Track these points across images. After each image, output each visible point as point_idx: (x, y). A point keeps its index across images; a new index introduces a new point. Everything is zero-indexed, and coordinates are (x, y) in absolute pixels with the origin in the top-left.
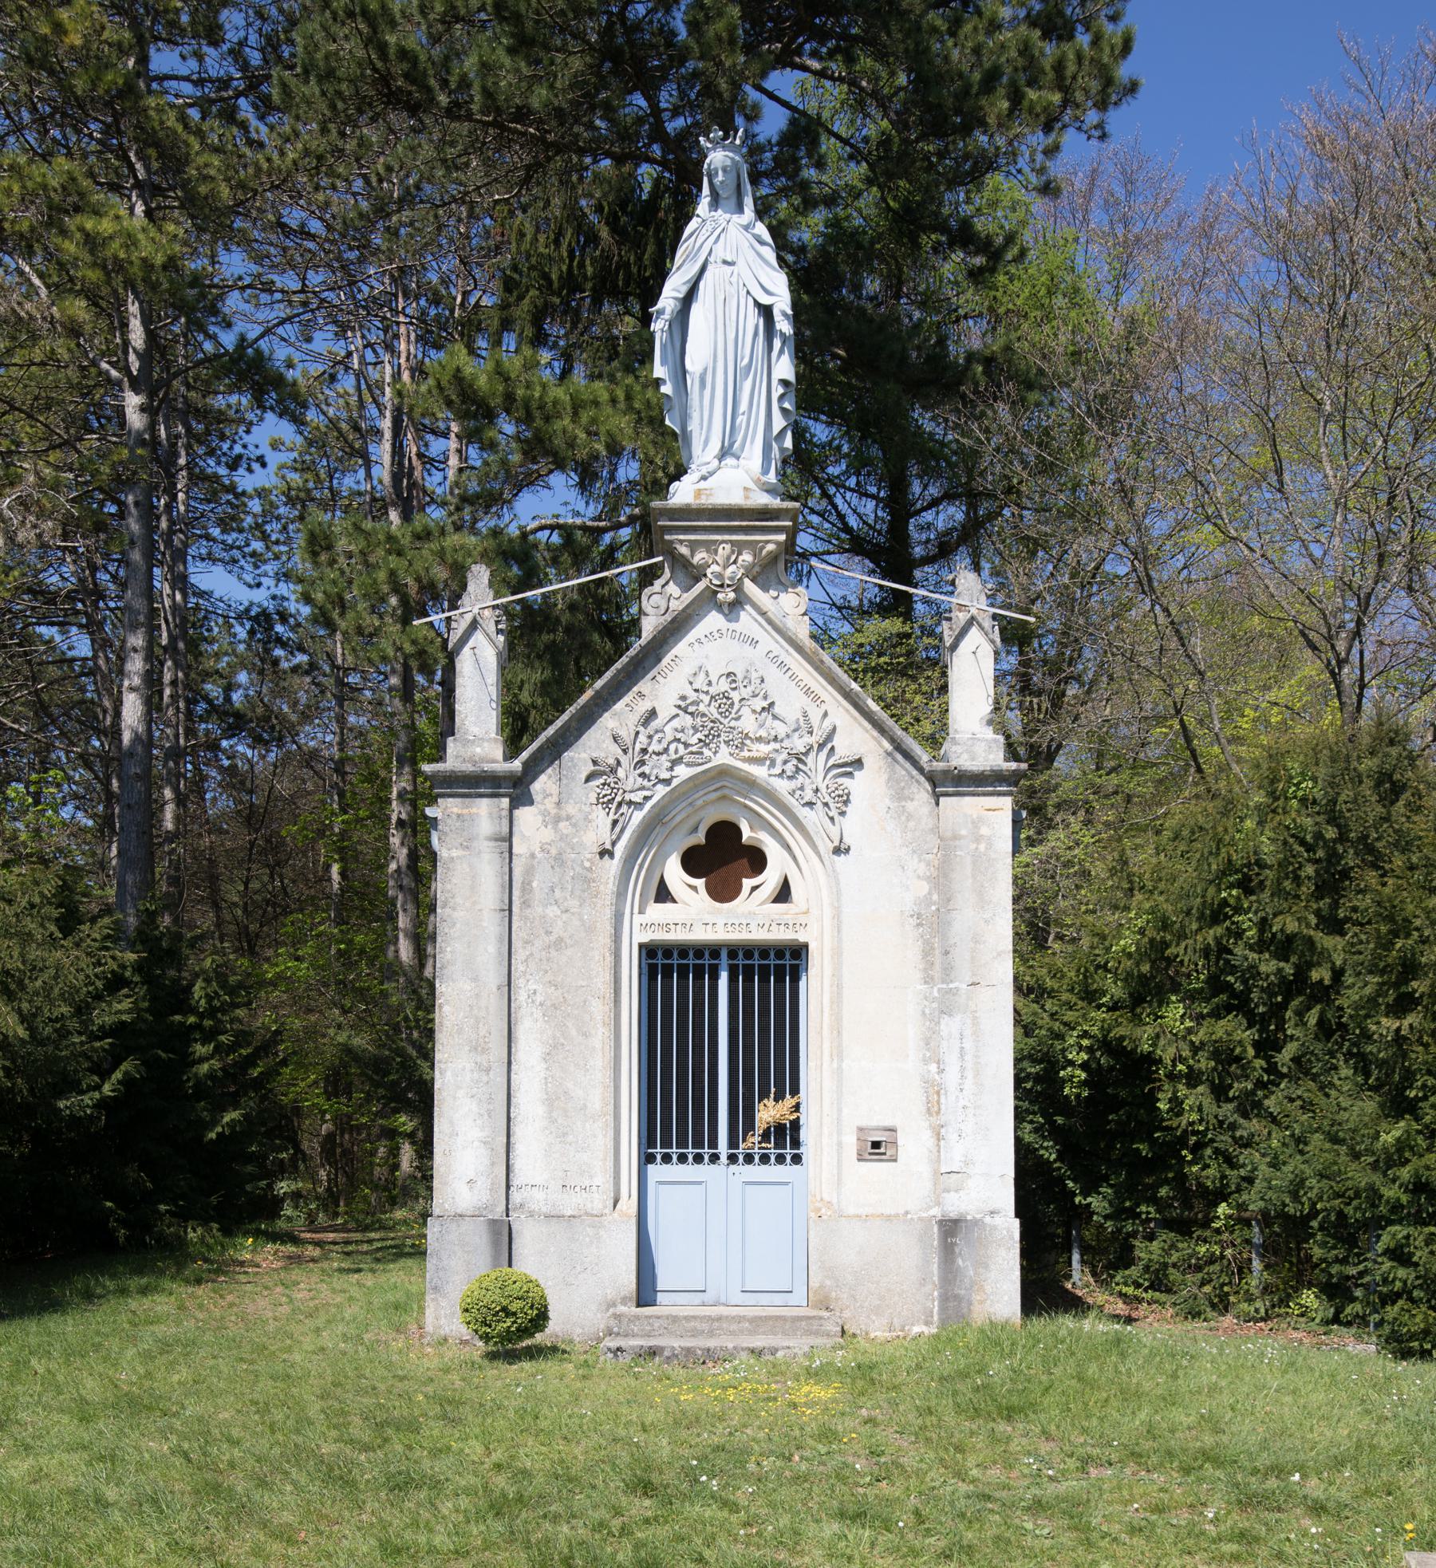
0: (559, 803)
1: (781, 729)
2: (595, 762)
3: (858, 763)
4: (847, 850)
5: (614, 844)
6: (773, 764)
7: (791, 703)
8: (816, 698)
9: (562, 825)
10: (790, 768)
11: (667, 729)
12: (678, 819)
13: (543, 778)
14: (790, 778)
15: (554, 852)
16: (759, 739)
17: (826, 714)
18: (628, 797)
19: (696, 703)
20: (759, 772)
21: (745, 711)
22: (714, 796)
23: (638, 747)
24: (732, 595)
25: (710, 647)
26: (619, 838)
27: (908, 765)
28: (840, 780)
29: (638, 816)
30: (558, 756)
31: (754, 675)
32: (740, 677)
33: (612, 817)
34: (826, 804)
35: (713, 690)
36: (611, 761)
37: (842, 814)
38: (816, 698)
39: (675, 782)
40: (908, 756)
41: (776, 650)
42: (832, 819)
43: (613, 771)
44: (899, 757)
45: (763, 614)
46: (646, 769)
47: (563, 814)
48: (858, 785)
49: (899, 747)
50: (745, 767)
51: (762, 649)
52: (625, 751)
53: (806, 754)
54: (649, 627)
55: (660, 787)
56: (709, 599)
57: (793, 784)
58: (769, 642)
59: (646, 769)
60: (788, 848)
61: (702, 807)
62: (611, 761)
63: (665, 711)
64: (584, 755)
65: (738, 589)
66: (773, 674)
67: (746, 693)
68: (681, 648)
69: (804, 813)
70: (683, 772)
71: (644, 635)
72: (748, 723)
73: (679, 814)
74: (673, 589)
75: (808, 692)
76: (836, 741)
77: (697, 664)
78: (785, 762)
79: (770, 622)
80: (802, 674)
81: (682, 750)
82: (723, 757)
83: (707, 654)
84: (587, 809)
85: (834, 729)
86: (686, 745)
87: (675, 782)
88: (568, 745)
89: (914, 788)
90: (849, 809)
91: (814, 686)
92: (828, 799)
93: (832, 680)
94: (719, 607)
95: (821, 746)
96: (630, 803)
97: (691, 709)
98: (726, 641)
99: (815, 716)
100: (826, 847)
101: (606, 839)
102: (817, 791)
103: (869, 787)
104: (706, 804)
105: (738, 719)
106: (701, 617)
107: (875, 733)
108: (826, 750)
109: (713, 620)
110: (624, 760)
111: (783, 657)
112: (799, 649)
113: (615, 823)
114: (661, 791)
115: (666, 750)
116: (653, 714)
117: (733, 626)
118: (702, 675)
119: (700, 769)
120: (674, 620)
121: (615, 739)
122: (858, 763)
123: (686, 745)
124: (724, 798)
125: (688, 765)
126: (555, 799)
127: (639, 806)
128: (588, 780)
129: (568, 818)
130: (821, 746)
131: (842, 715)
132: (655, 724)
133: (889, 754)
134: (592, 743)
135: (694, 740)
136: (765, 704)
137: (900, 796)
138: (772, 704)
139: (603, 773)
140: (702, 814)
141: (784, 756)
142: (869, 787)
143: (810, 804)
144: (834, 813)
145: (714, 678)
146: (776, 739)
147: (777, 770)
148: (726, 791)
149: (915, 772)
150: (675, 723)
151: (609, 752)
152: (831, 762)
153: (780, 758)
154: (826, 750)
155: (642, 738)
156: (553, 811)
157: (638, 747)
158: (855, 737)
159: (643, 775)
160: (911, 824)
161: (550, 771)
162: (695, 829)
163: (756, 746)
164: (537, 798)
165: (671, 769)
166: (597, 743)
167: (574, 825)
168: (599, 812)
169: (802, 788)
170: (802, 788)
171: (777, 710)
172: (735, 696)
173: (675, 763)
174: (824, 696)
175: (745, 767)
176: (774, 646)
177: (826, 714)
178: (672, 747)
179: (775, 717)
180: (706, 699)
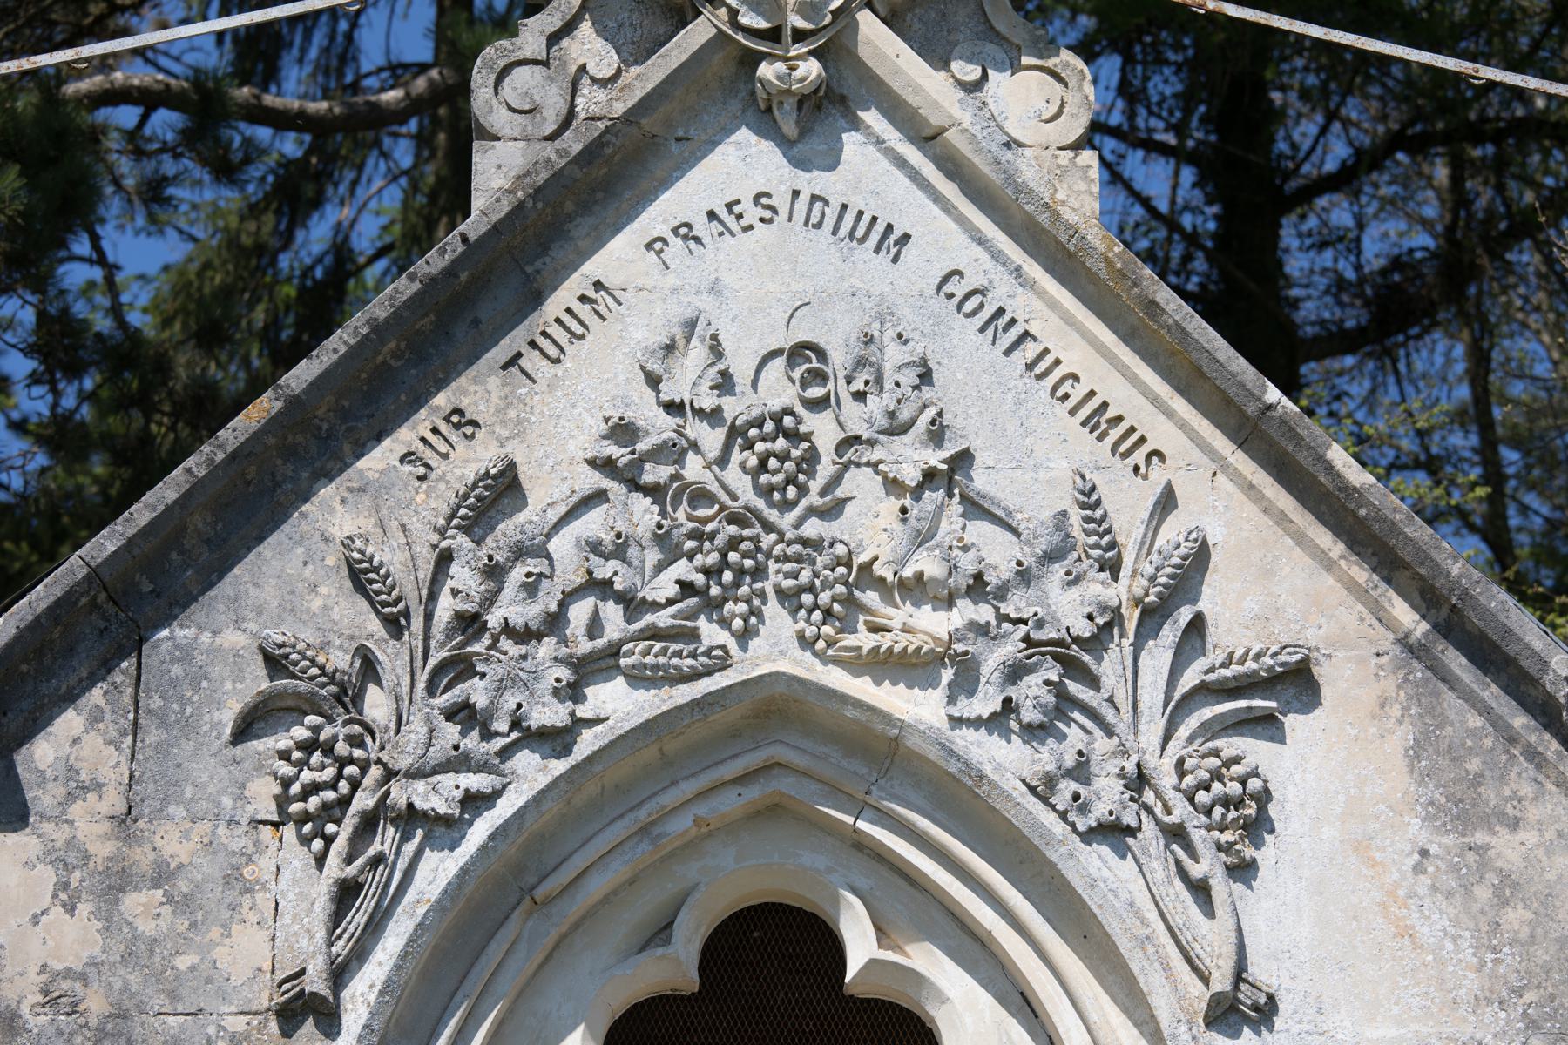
0: (125, 821)
1: (997, 552)
2: (275, 663)
3: (1296, 682)
4: (1265, 1013)
5: (340, 974)
6: (966, 682)
7: (1033, 462)
8: (1131, 445)
9: (134, 902)
10: (1033, 691)
11: (562, 546)
12: (597, 886)
13: (69, 722)
14: (1035, 733)
15: (96, 1005)
16: (915, 589)
17: (1167, 502)
18: (399, 794)
19: (673, 452)
20: (918, 708)
21: (861, 485)
22: (731, 803)
23: (446, 607)
24: (811, 69)
25: (729, 257)
26: (360, 954)
27: (1491, 693)
28: (1231, 745)
29: (438, 871)
30: (136, 644)
31: (894, 355)
32: (839, 360)
33: (334, 867)
34: (1176, 834)
35: (733, 408)
36: (340, 660)
37: (1243, 871)
38: (1131, 445)
39: (587, 743)
40: (1492, 656)
41: (978, 267)
42: (1201, 890)
43: (348, 696)
44: (1456, 662)
45: (929, 139)
46: (477, 692)
47: (142, 858)
48: (1301, 765)
49: (1453, 622)
50: (861, 688)
51: (922, 265)
52: (395, 626)
53: (1097, 642)
54: (496, 174)
55: (525, 760)
56: (726, 90)
57: (1045, 757)
58: (946, 237)
59: (477, 692)
60: (1025, 1006)
61: (691, 847)
62: (340, 660)
63: (555, 467)
64: (232, 638)
65: (835, 46)
66: (964, 354)
67: (857, 418)
68: (618, 257)
69: (1097, 872)
70: (617, 704)
71: (478, 203)
72: (871, 526)
73: (601, 871)
74: (590, 49)
75: (1098, 419)
76: (1212, 599)
77: (678, 311)
78: (1015, 673)
79: (953, 166)
80: (1073, 356)
81: (612, 613)
82: (776, 649)
83: (722, 270)
84: (238, 841)
85: (1199, 558)
86: (632, 605)
87: (587, 743)
88: (174, 605)
89: (1522, 779)
90: (1265, 856)
91: (1122, 398)
92: (1181, 811)
93: (1192, 380)
94: (763, 116)
95: (1153, 616)
96: (411, 817)
97: (654, 473)
98: (787, 235)
99: (1127, 505)
100: (1176, 997)
101: (307, 945)
102: (1139, 781)
103: (1338, 772)
104: (707, 834)
105: (832, 511)
106: (696, 150)
107: (1361, 574)
108: (1169, 634)
109: (742, 162)
110: (393, 659)
111: (1003, 291)
112: (1064, 261)
113: (346, 893)
114: (532, 773)
115: (554, 623)
116: (503, 489)
117: (813, 182)
118: (697, 354)
119: (685, 693)
120: (591, 153)
121: (361, 576)
122: (1296, 682)
123: (632, 605)
124: (773, 811)
125: (639, 678)
126: (113, 801)
127: (444, 829)
128: (245, 730)
129: (162, 875)
130: (1153, 616)
131: (1225, 505)
132: (510, 528)
133: (1413, 650)
134: (268, 594)
135: (664, 587)
136: (936, 458)
137: (1463, 810)
138: (963, 460)
139: (297, 708)
140: (690, 871)
141: (1010, 648)
142: (1338, 772)
143: (1114, 833)
144: (1207, 865)
145: (741, 365)
146: (978, 587)
147: (985, 703)
148: (785, 785)
149: (1520, 721)
150: (593, 524)
151: (334, 623)
152: (1191, 677)
153: (993, 659)
154: (1169, 634)
155: (463, 576)
156: (102, 850)
157: (446, 607)
158: (1275, 582)
159: (462, 713)
160: (1516, 918)
161: (96, 695)
162: (662, 932)
163: (898, 614)
164: (42, 798)
165: (573, 691)
166: (289, 592)
167: (183, 904)
168: (291, 852)
169: (1081, 771)
170: (1081, 771)
171: (980, 480)
172: (823, 430)
173: (588, 670)
174: (1161, 434)
175: (861, 688)
176: (966, 255)
177: (1167, 502)
178: (580, 612)
179: (975, 508)
180: (711, 439)
